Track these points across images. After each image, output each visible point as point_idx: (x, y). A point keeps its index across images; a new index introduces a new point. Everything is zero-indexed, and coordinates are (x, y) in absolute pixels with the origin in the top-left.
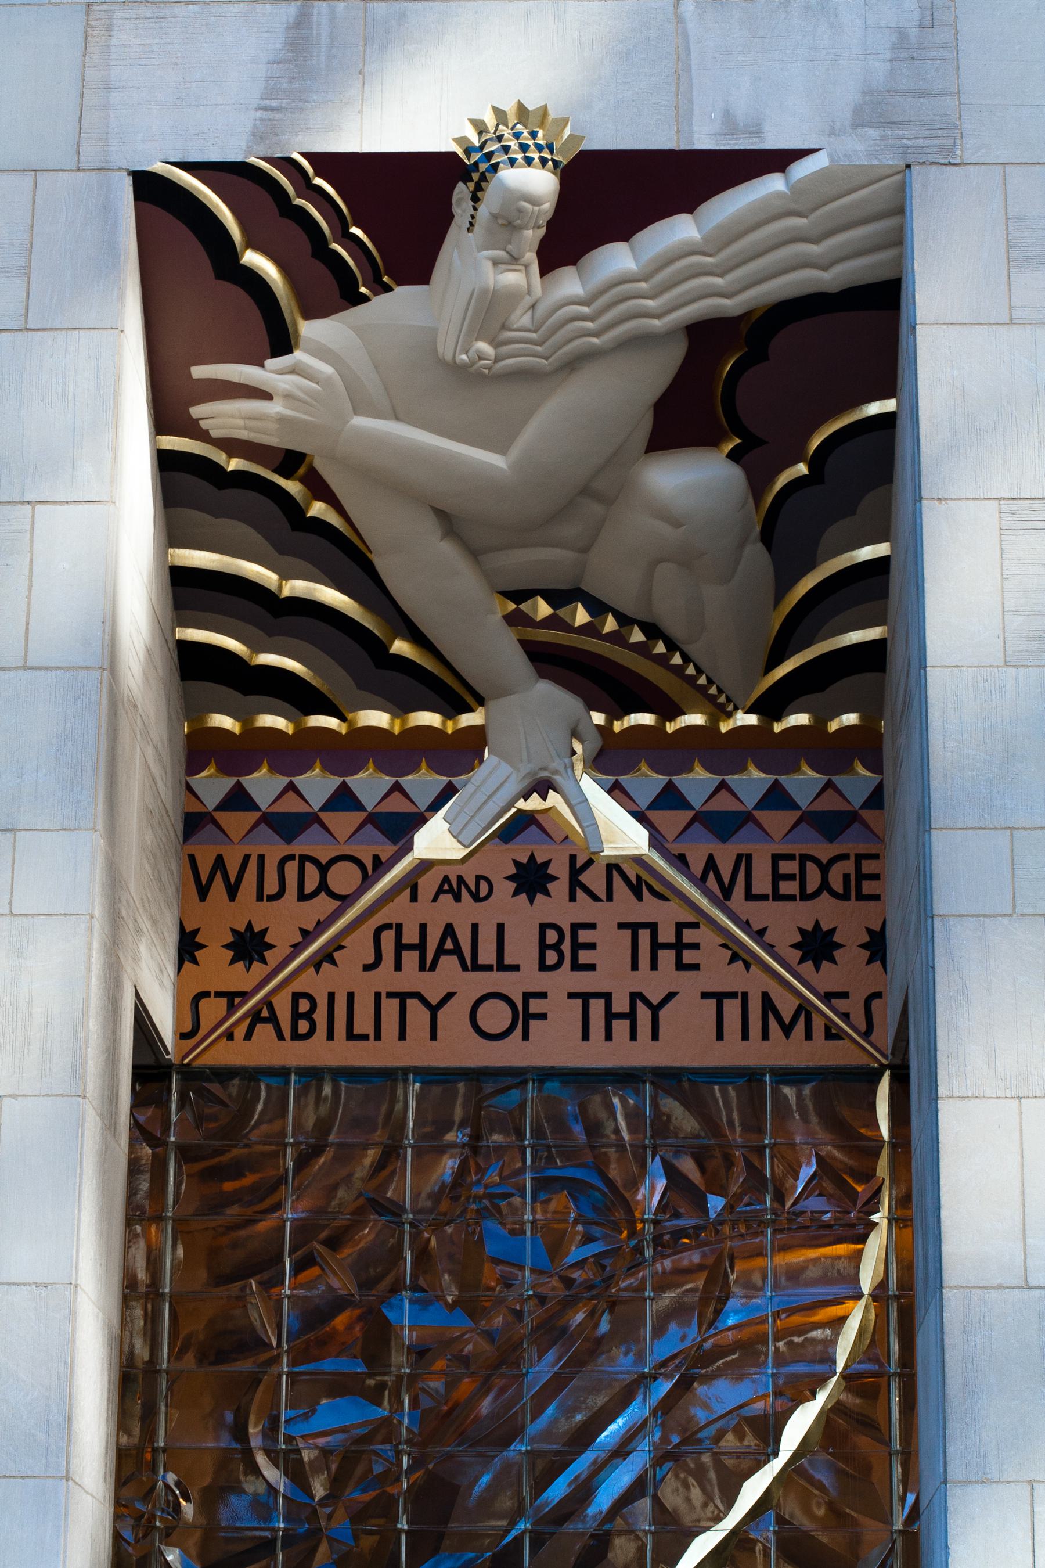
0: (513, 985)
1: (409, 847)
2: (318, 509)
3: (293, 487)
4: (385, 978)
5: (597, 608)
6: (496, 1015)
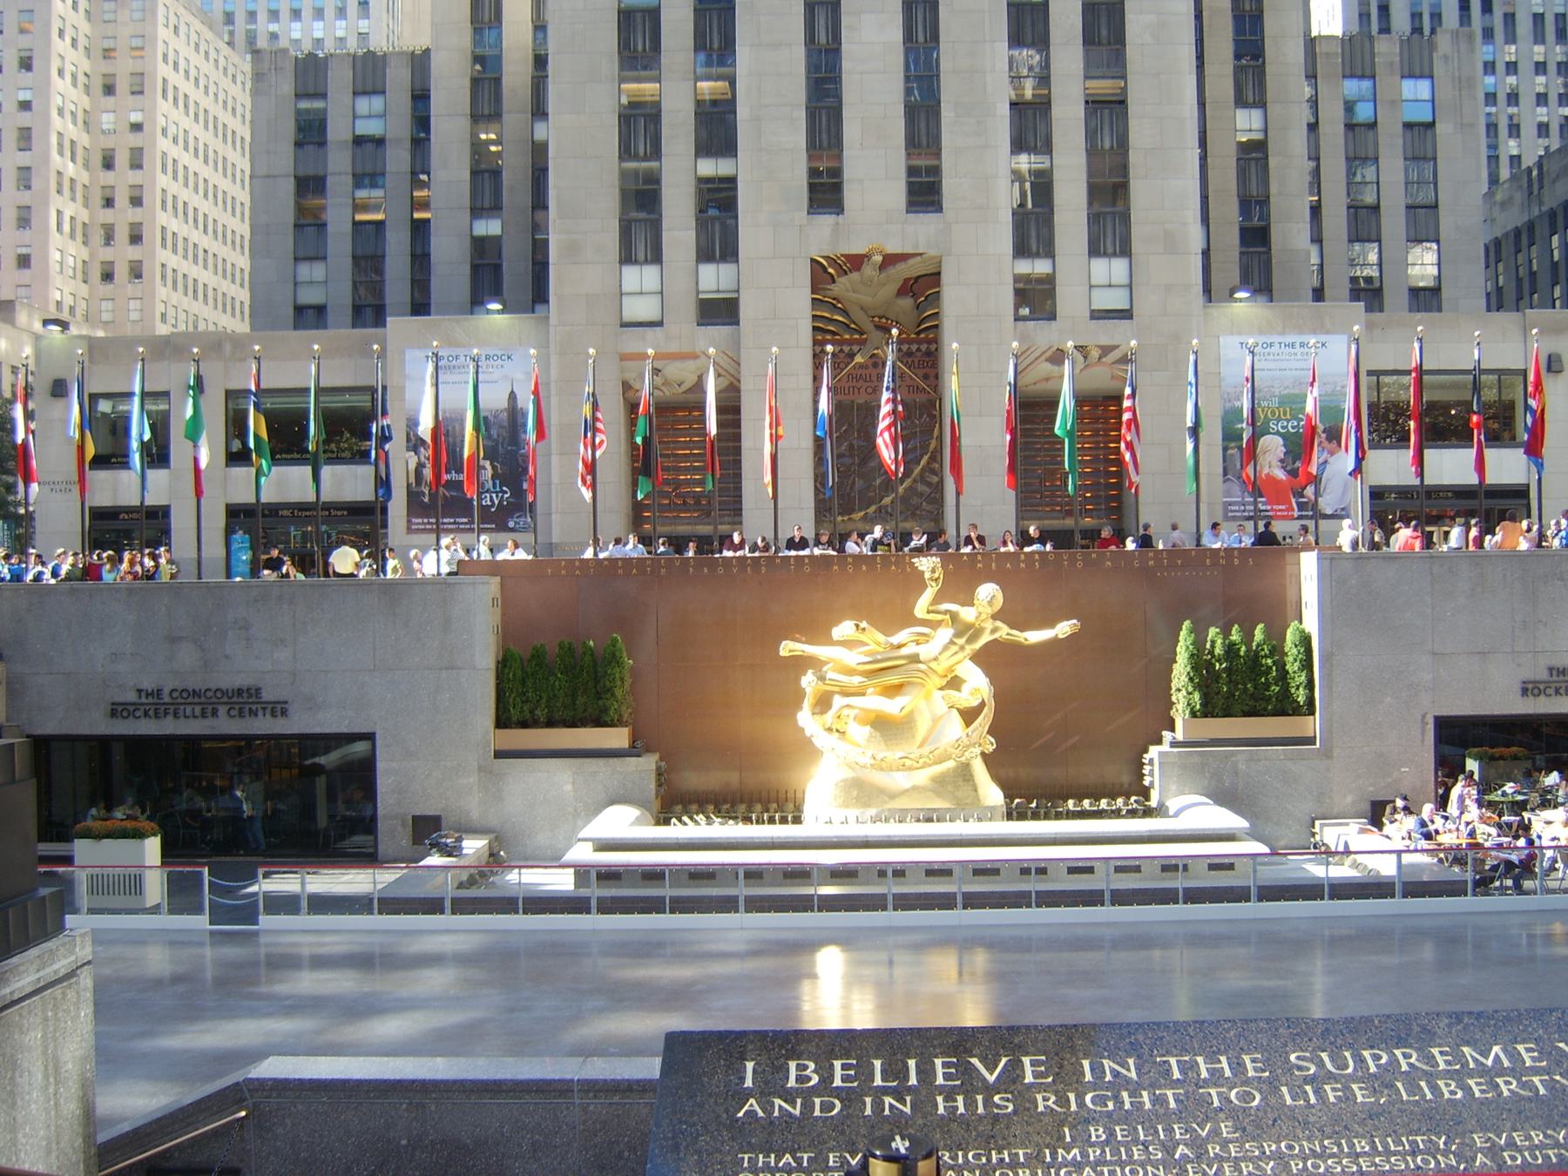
0: (873, 385)
1: (853, 360)
2: (840, 305)
3: (834, 302)
4: (850, 384)
5: (887, 319)
6: (870, 390)
